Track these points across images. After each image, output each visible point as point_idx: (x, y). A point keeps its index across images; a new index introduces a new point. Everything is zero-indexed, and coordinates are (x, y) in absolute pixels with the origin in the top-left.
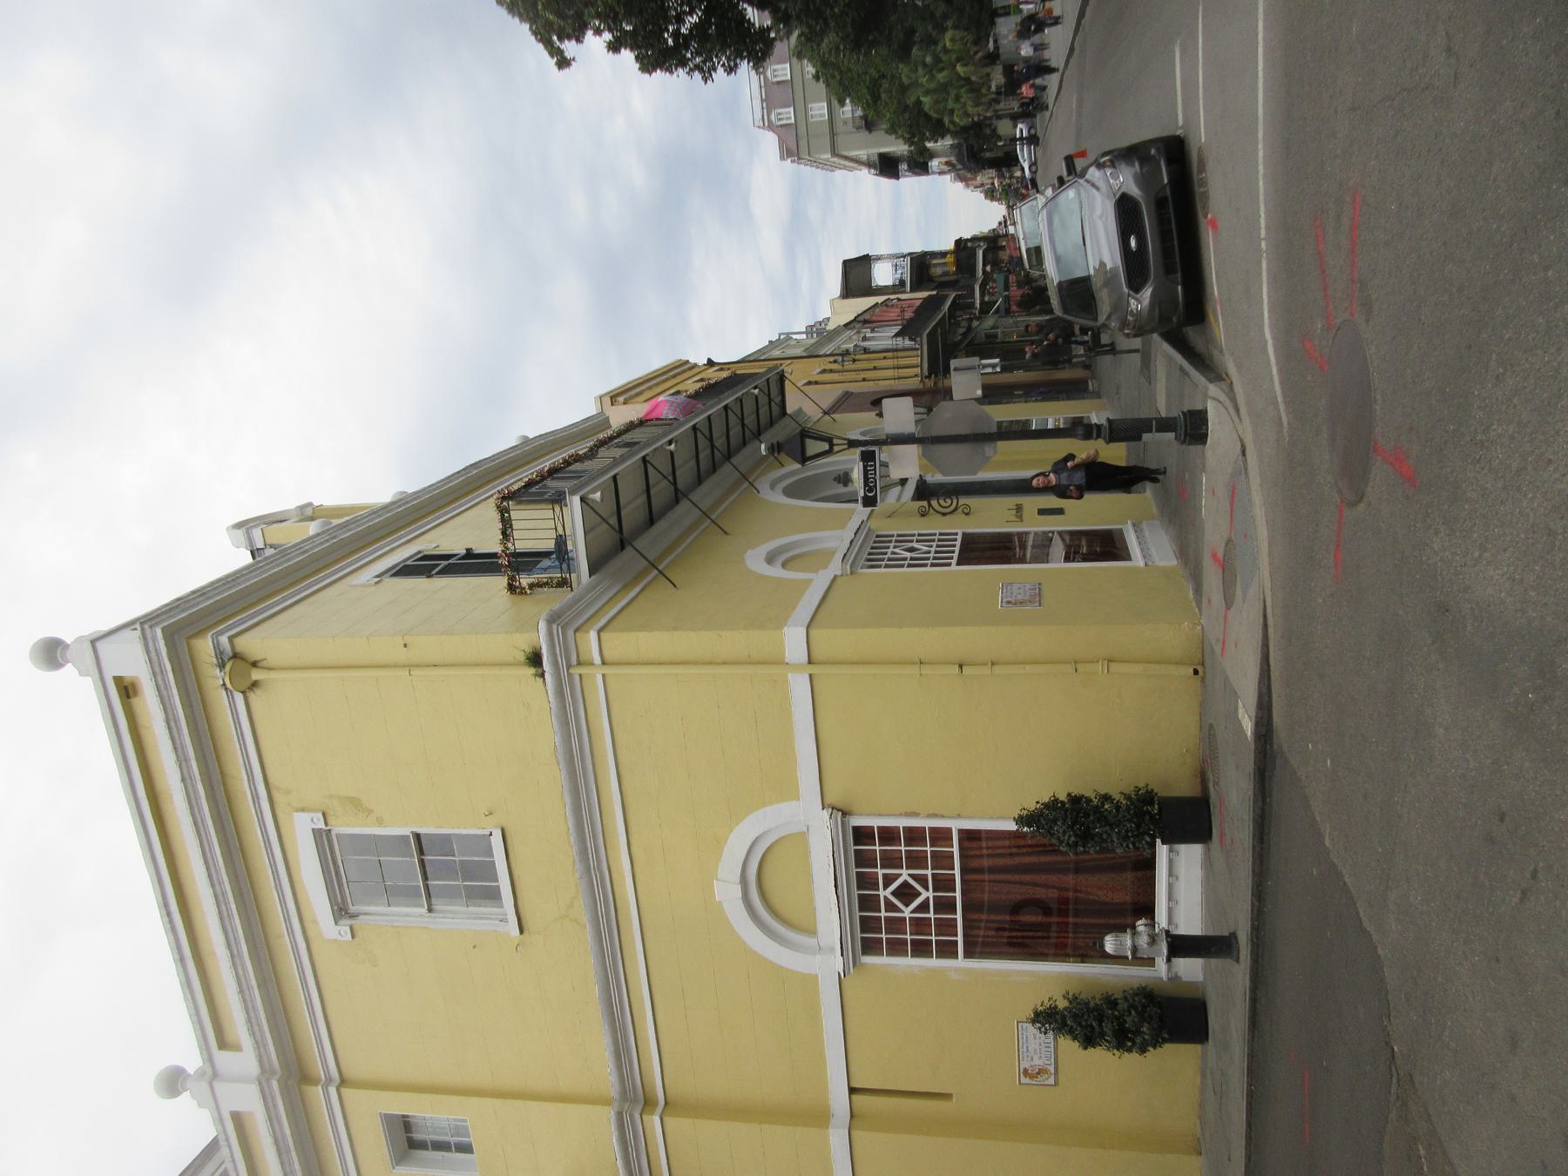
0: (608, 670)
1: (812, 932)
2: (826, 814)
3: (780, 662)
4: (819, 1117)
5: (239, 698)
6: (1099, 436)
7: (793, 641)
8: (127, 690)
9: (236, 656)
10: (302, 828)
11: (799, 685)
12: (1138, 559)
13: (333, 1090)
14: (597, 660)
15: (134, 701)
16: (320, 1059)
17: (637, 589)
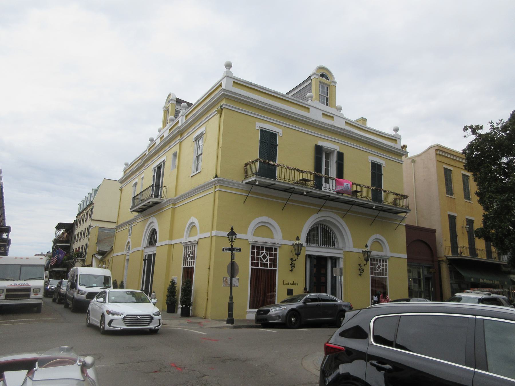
0: (213, 194)
1: (189, 237)
2: (197, 239)
3: (212, 229)
4: (171, 238)
7: (214, 233)
8: (221, 85)
9: (222, 109)
10: (202, 129)
11: (208, 234)
12: (249, 310)
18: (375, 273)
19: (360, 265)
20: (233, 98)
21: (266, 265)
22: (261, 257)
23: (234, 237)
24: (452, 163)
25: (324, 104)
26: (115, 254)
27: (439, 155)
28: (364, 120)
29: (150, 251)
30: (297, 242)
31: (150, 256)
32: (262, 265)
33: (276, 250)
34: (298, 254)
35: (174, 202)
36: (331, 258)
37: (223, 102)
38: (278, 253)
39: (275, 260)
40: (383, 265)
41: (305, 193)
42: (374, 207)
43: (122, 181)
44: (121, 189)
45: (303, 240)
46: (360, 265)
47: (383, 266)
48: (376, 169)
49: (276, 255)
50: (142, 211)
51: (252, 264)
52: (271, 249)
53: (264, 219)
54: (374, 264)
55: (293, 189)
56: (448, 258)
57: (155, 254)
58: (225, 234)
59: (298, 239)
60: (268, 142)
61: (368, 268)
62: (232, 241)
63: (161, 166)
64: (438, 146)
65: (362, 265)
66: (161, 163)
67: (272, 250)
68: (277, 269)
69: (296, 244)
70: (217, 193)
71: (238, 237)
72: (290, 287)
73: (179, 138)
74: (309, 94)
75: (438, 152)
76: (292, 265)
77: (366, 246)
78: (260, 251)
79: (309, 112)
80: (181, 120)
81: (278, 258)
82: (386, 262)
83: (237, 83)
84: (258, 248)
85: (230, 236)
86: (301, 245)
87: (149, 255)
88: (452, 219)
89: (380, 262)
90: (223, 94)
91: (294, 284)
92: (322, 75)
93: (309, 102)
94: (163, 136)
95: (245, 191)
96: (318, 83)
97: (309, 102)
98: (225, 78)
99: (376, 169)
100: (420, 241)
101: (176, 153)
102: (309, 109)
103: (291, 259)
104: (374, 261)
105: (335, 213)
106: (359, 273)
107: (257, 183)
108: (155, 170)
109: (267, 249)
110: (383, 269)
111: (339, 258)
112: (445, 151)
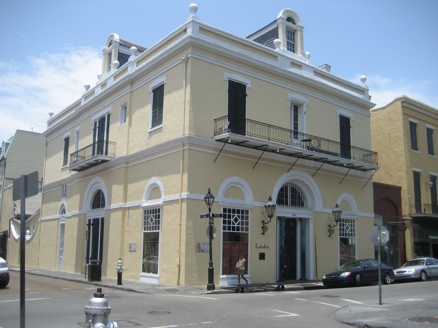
1: (150, 199)
5: (181, 61)
6: (210, 266)
8: (185, 31)
12: (222, 276)
13: (129, 91)
14: (184, 149)
15: (184, 33)
16: (136, 86)
17: (214, 152)
18: (343, 233)
19: (329, 226)
20: (201, 47)
21: (238, 229)
22: (232, 220)
23: (212, 199)
24: (417, 115)
25: (291, 51)
26: (43, 218)
27: (405, 107)
28: (328, 67)
29: (98, 214)
30: (270, 203)
31: (96, 221)
32: (234, 228)
33: (247, 212)
34: (271, 217)
35: (127, 160)
36: (300, 219)
37: (190, 51)
38: (249, 215)
39: (247, 224)
40: (351, 225)
41: (278, 151)
42: (345, 165)
43: (48, 134)
44: (47, 144)
45: (274, 202)
46: (329, 226)
47: (351, 227)
48: (345, 123)
49: (247, 218)
50: (81, 169)
51: (224, 228)
52: (243, 211)
53: (235, 179)
54: (343, 224)
55: (266, 147)
56: (413, 216)
57: (103, 219)
58: (202, 197)
59: (270, 199)
60: (237, 94)
61: (337, 229)
62: (209, 205)
63: (104, 118)
64: (405, 98)
65: (332, 225)
66: (105, 114)
67: (243, 213)
68: (249, 232)
69: (269, 206)
70: (186, 153)
71: (215, 200)
72: (262, 251)
73: (129, 87)
74: (276, 40)
75: (404, 105)
76: (264, 229)
77: (337, 206)
78: (232, 214)
79: (277, 61)
80: (132, 69)
81: (249, 221)
82: (354, 222)
83: (203, 29)
84: (229, 211)
85: (207, 199)
86: (274, 206)
87: (94, 220)
88: (417, 176)
89: (349, 222)
90: (190, 42)
91: (265, 247)
92: (289, 19)
93: (277, 50)
94: (106, 83)
95: (215, 149)
96: (285, 28)
97: (277, 50)
98: (191, 23)
99: (345, 123)
100: (386, 199)
101: (126, 104)
102: (277, 57)
103: (263, 222)
104: (343, 222)
105: (306, 171)
106: (329, 234)
107: (229, 141)
108: (95, 123)
109: (238, 211)
110: (351, 229)
111: (308, 219)
112: (411, 103)
